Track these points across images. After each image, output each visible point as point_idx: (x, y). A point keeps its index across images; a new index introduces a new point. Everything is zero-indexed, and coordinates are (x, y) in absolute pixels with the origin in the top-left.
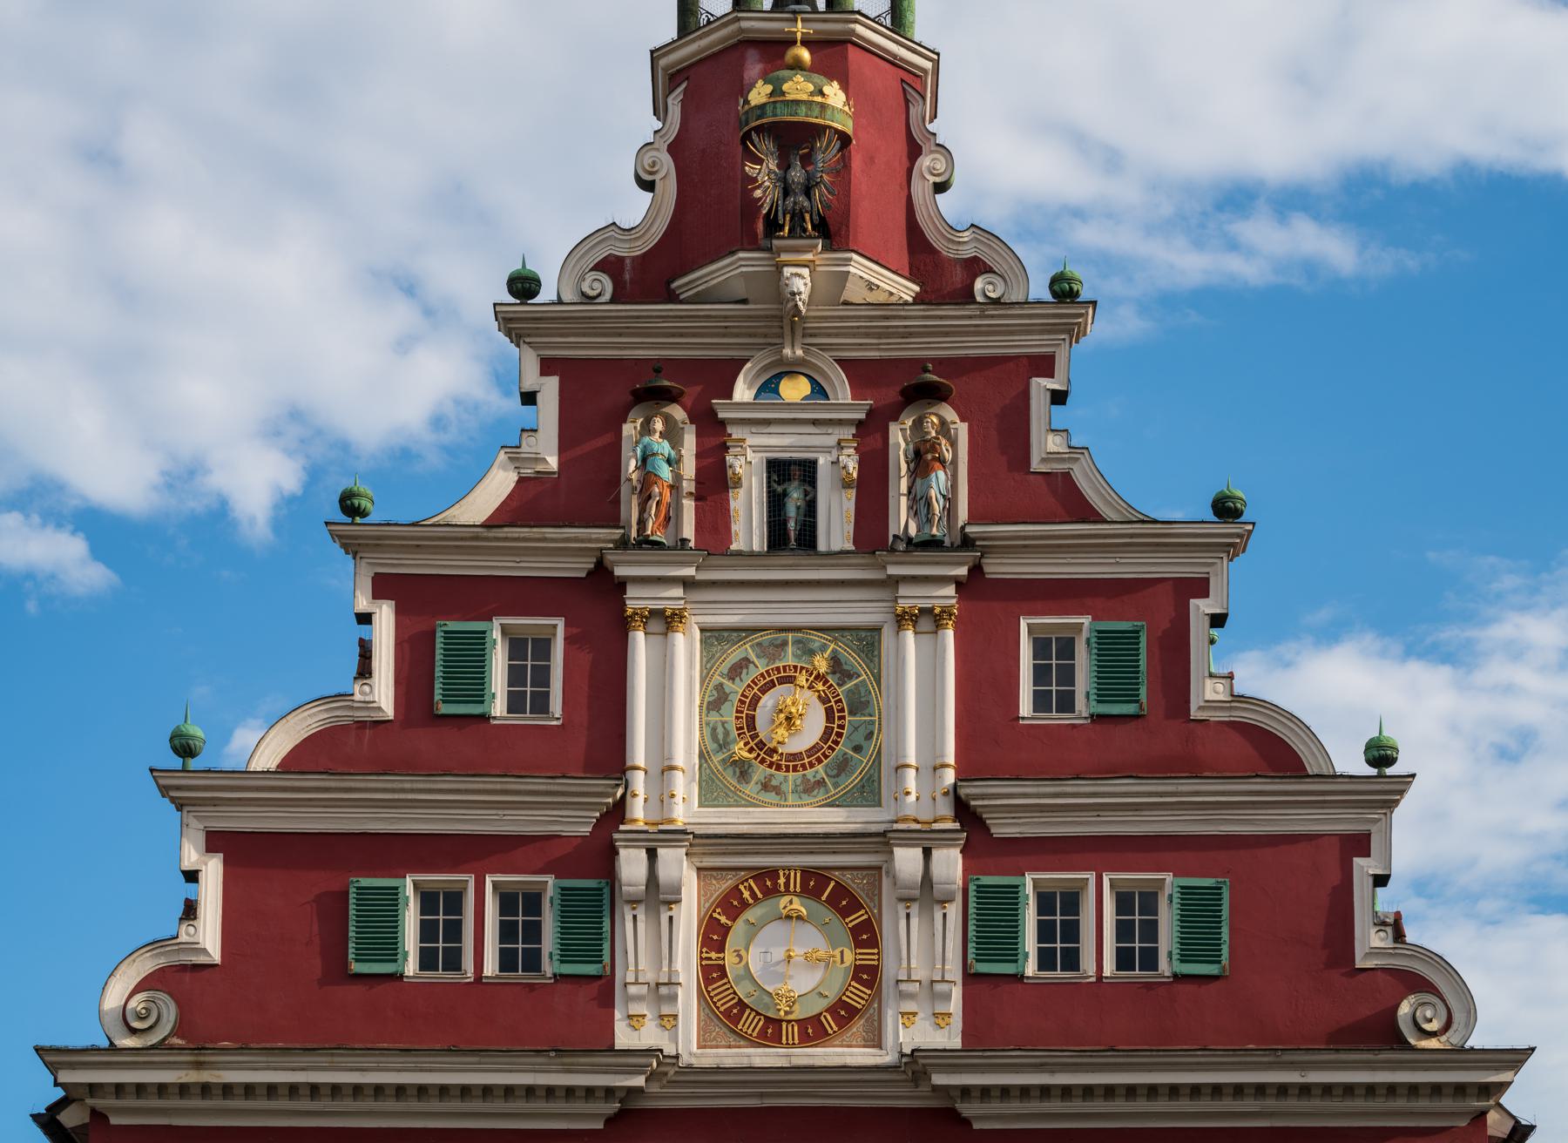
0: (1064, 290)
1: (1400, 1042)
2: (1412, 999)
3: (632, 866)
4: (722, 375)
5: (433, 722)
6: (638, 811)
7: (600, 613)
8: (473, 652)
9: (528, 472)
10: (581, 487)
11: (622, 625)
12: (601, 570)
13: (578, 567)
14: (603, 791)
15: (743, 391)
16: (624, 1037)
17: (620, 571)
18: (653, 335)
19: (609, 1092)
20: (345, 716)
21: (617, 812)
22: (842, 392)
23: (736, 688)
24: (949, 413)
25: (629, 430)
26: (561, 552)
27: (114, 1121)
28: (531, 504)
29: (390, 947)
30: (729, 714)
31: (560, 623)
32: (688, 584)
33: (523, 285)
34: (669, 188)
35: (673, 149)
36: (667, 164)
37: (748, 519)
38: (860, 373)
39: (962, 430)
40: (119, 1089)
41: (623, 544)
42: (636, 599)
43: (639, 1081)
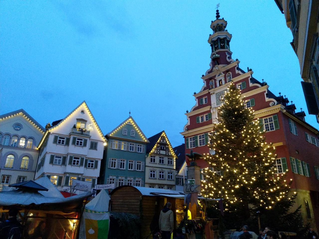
0: (237, 60)
1: (270, 106)
2: (271, 103)
3: (212, 112)
4: (215, 76)
5: (200, 106)
6: (212, 107)
7: (209, 95)
8: (202, 100)
9: (205, 87)
10: (208, 87)
11: (210, 95)
12: (209, 91)
13: (207, 92)
14: (209, 107)
15: (216, 76)
16: (213, 123)
17: (209, 92)
18: (212, 75)
19: (212, 127)
20: (195, 107)
21: (211, 108)
22: (223, 73)
23: (218, 97)
24: (230, 72)
25: (210, 82)
26: (206, 92)
27: (186, 136)
28: (205, 89)
29: (199, 121)
30: (218, 98)
31: (207, 96)
32: (214, 91)
33: (203, 76)
34: (212, 66)
35: (212, 63)
36: (211, 64)
37: (218, 84)
38: (224, 72)
39: (231, 73)
40: (185, 134)
41: (210, 89)
42: (211, 93)
43: (213, 126)
